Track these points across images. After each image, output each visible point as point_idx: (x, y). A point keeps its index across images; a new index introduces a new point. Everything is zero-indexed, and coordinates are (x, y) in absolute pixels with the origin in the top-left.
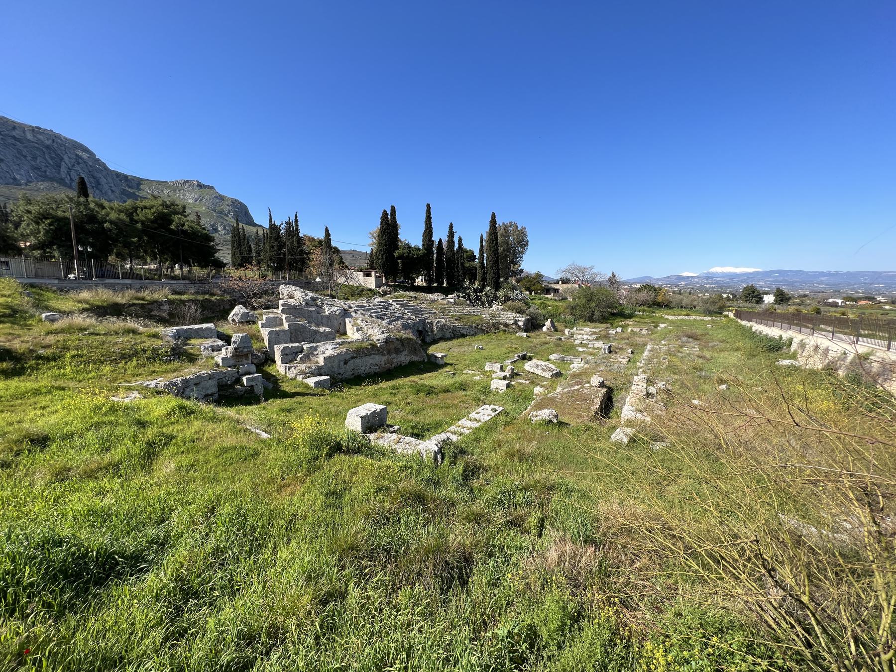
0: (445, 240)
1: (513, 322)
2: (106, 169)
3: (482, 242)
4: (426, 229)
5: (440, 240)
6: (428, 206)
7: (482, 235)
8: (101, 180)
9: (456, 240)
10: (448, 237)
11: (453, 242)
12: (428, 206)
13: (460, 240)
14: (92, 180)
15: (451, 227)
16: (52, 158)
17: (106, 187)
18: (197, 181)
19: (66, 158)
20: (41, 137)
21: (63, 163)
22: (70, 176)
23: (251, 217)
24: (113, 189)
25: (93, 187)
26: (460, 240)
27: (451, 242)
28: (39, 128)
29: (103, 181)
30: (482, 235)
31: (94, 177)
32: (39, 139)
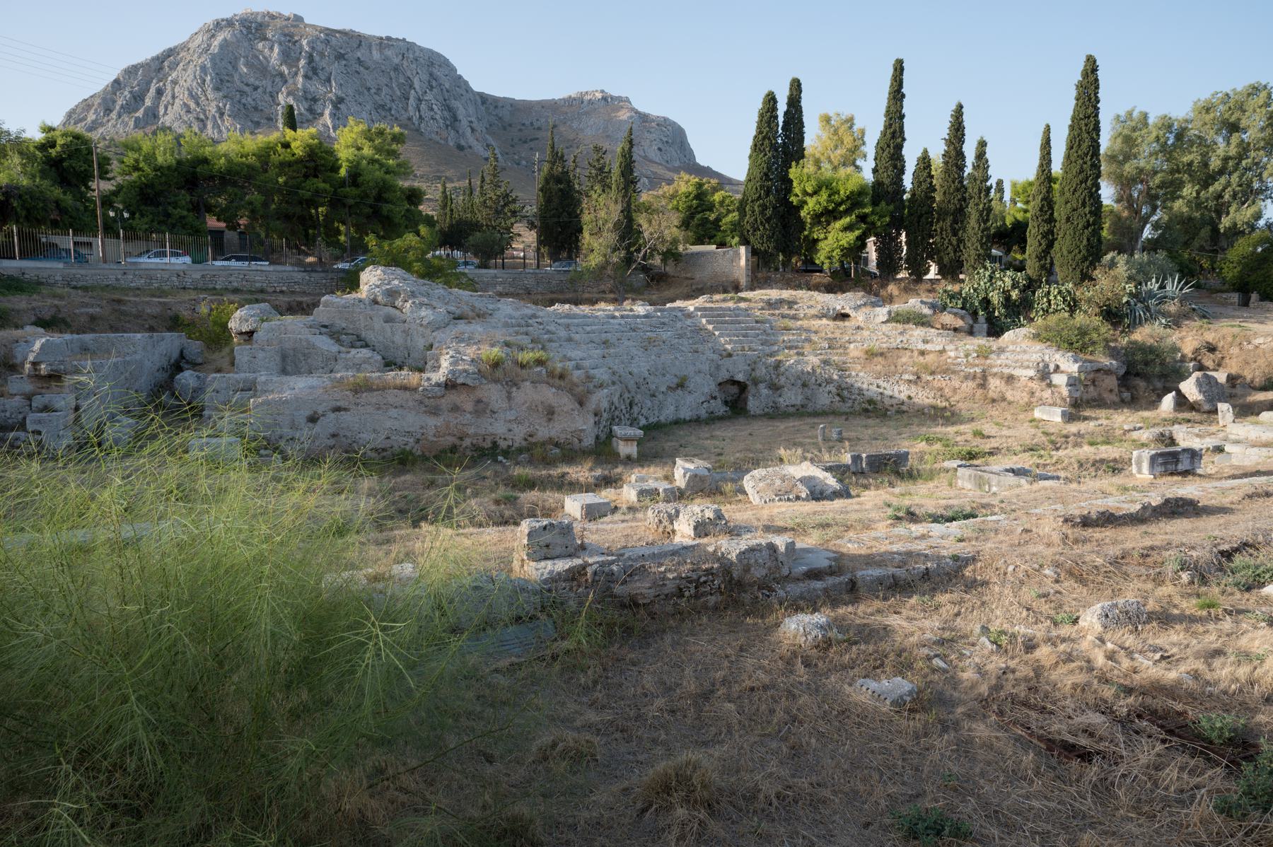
0: (937, 152)
1: (1031, 373)
2: (468, 89)
3: (1046, 145)
4: (886, 128)
5: (926, 151)
6: (899, 68)
7: (1048, 130)
8: (459, 112)
9: (970, 151)
10: (949, 142)
11: (960, 155)
12: (899, 68)
13: (982, 144)
14: (446, 114)
15: (958, 113)
16: (400, 86)
17: (464, 123)
18: (602, 91)
19: (417, 84)
20: (388, 53)
21: (413, 92)
22: (419, 111)
23: (691, 152)
24: (474, 125)
25: (447, 126)
26: (982, 144)
27: (955, 154)
28: (389, 38)
29: (461, 113)
30: (1048, 130)
31: (449, 109)
32: (386, 59)
